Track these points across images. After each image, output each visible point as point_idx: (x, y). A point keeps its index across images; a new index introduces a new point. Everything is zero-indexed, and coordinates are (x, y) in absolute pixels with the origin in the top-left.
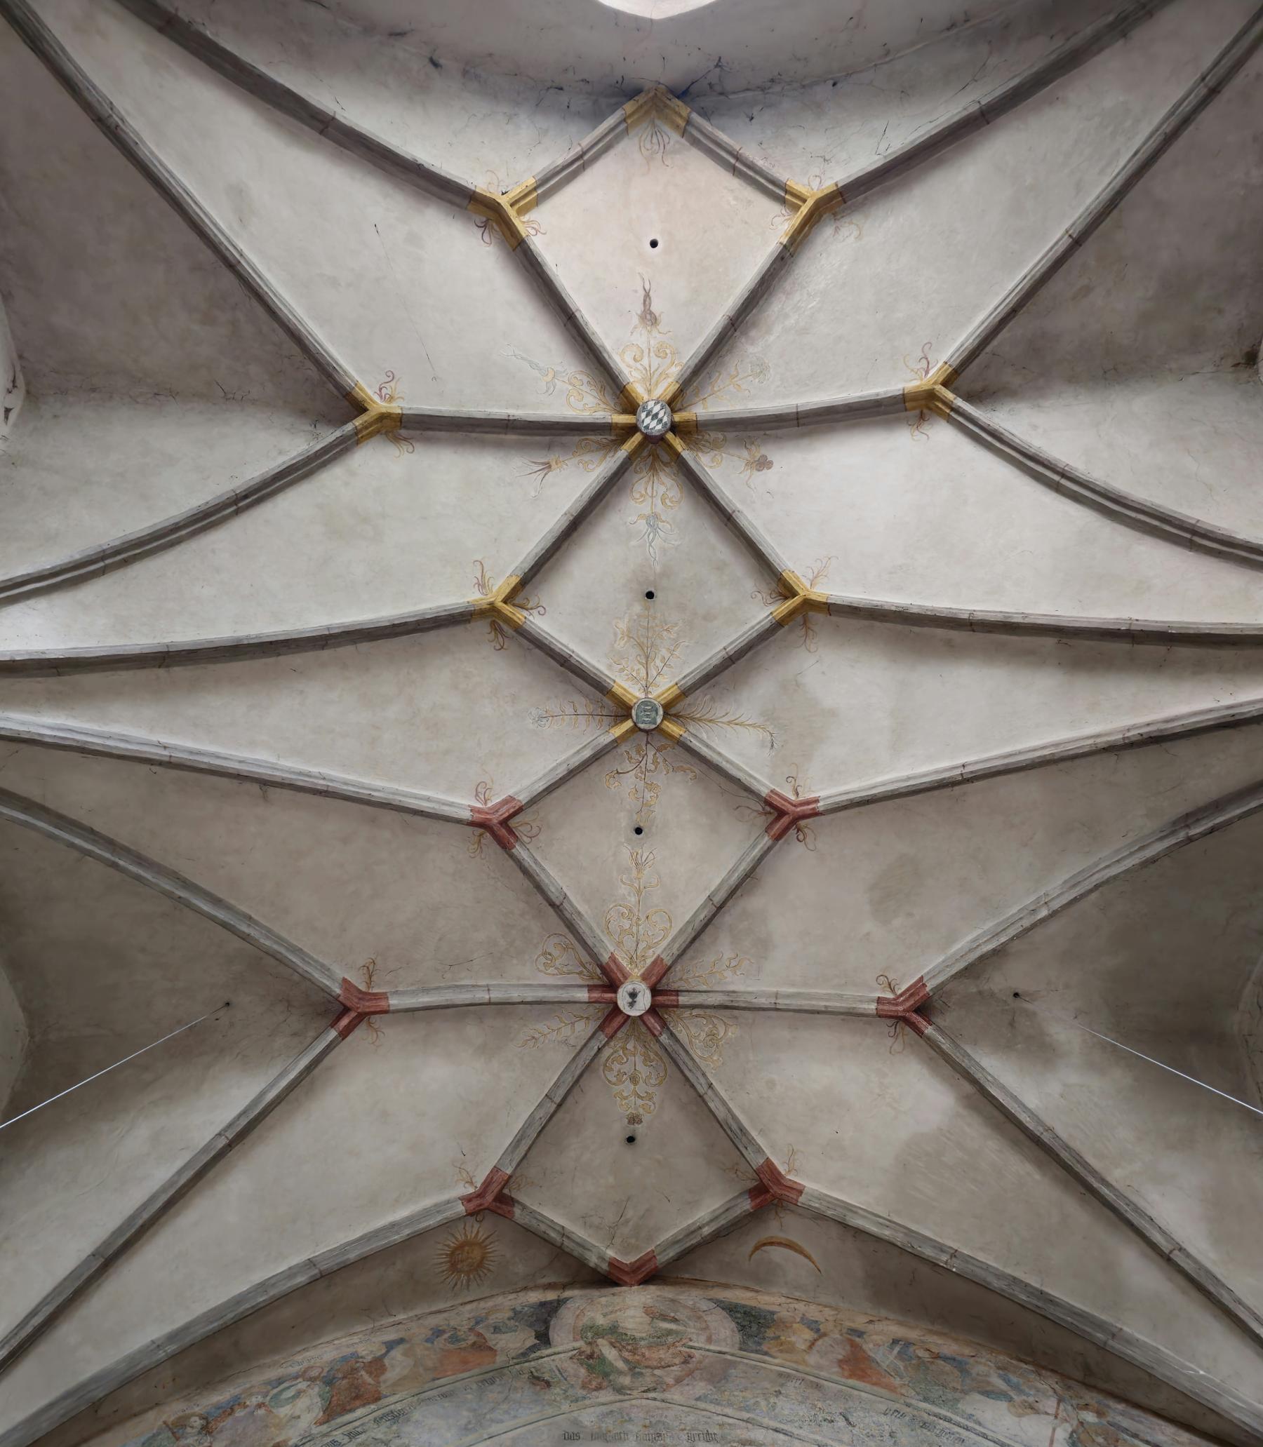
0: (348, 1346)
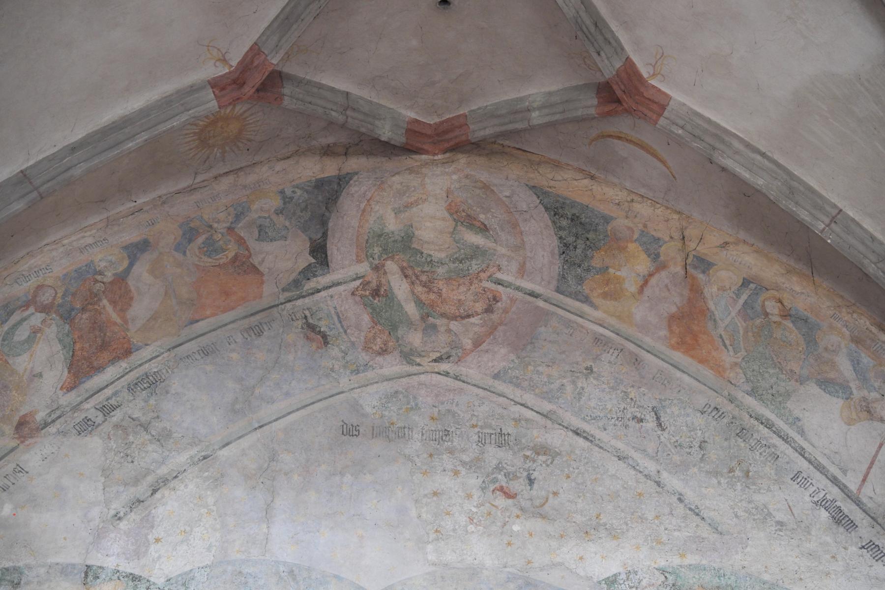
0: (81, 250)
